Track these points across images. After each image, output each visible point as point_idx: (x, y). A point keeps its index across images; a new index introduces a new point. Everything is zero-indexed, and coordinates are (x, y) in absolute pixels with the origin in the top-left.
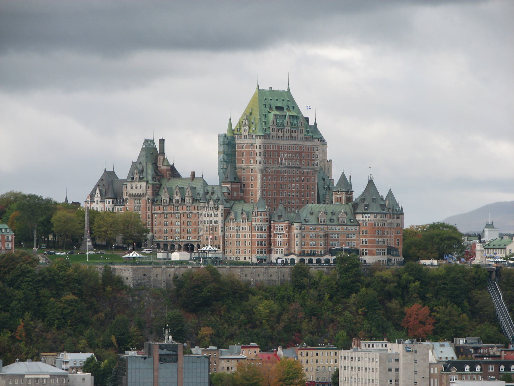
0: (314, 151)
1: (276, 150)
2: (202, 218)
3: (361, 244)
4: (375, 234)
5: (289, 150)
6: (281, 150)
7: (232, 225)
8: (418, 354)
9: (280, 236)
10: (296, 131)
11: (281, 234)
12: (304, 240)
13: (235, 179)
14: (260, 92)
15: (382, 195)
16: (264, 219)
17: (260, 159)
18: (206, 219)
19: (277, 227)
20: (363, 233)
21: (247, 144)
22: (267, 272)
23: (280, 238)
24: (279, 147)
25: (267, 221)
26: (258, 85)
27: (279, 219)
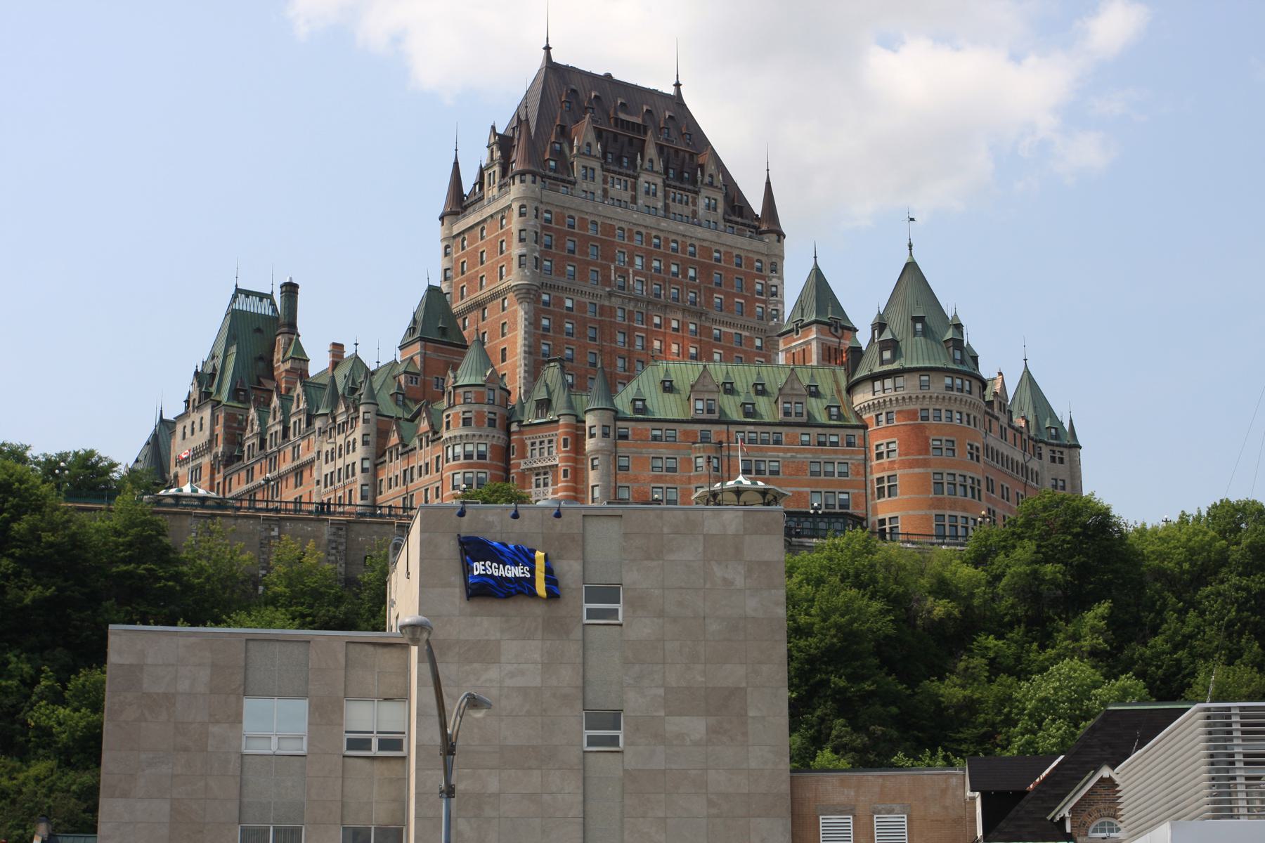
0: (764, 273)
1: (599, 236)
2: (320, 468)
4: (927, 452)
5: (652, 248)
6: (617, 240)
7: (394, 468)
9: (542, 477)
10: (690, 200)
11: (545, 471)
15: (956, 315)
16: (480, 415)
17: (524, 251)
18: (327, 469)
19: (533, 444)
20: (879, 456)
21: (492, 216)
22: (343, 540)
23: (542, 489)
24: (609, 230)
26: (548, 48)
27: (537, 418)
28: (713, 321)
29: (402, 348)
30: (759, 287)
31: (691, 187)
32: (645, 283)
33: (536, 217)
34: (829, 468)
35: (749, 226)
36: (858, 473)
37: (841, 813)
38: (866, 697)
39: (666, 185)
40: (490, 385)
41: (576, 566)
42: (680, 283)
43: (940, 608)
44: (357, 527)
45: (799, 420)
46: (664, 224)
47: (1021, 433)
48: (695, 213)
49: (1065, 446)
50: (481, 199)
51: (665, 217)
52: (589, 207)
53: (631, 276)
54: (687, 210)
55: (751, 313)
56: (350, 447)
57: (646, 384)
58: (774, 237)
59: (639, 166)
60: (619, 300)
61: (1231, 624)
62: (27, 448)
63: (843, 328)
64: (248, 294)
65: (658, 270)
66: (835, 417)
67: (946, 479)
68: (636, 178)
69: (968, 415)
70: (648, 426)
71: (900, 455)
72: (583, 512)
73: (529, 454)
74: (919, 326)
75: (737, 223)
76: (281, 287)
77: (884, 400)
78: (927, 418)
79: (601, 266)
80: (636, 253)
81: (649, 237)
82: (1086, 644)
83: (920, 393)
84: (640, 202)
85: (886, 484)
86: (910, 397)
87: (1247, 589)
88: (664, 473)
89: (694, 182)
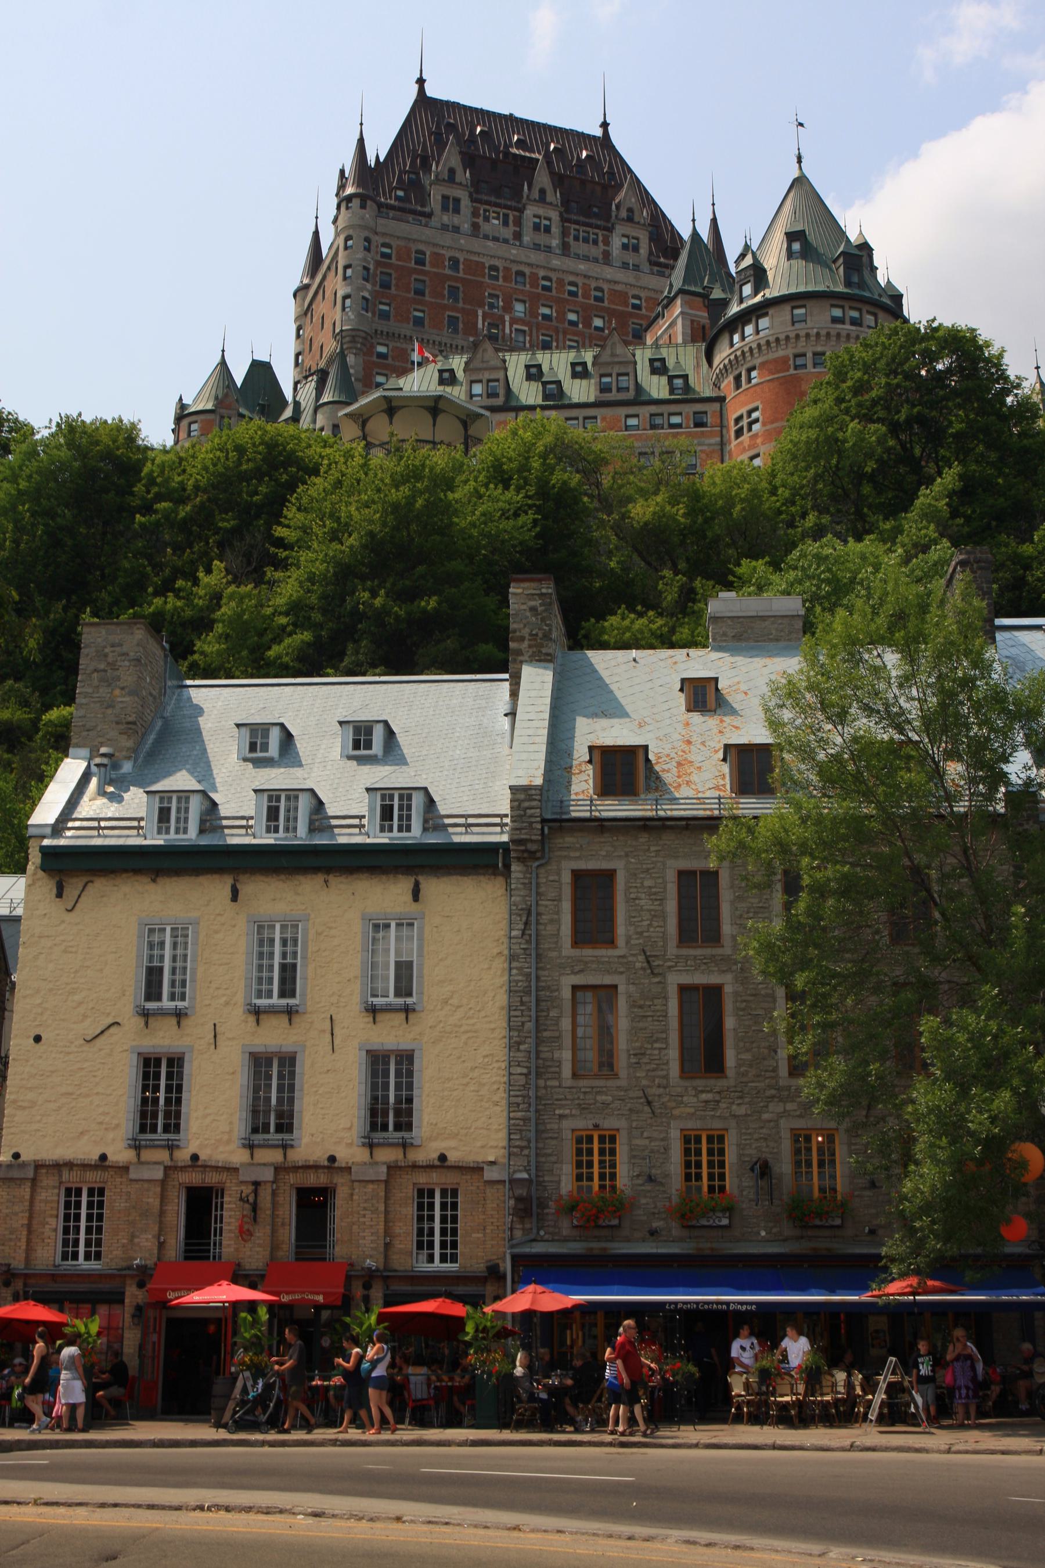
1: (461, 274)
10: (600, 238)
20: (739, 433)
24: (474, 267)
26: (421, 81)
32: (528, 332)
33: (367, 249)
39: (563, 220)
46: (556, 262)
48: (607, 255)
52: (447, 239)
53: (507, 324)
54: (596, 251)
59: (525, 196)
65: (545, 317)
66: (680, 391)
68: (521, 211)
71: (764, 424)
74: (796, 246)
77: (743, 352)
80: (515, 296)
81: (534, 277)
83: (790, 330)
84: (526, 239)
86: (777, 340)
89: (608, 217)
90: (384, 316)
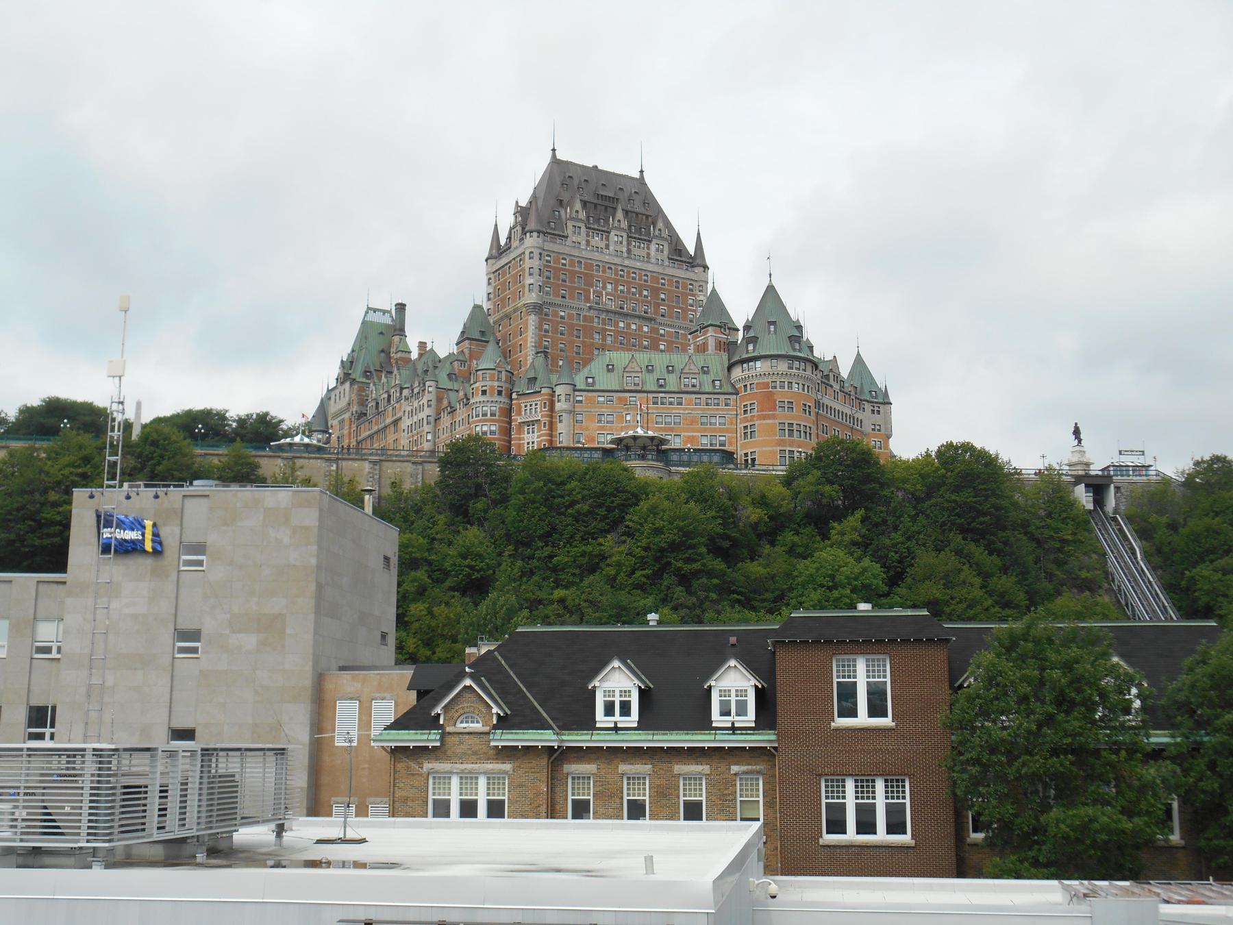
3: (741, 440)
5: (619, 277)
8: (217, 572)
9: (531, 427)
11: (533, 423)
12: (581, 428)
13: (482, 333)
14: (557, 165)
17: (532, 281)
18: (409, 422)
19: (526, 406)
20: (745, 412)
21: (514, 259)
24: (589, 266)
25: (500, 393)
26: (554, 150)
28: (660, 324)
29: (457, 344)
30: (691, 301)
31: (647, 238)
33: (540, 259)
34: (713, 420)
35: (685, 262)
36: (732, 424)
37: (351, 699)
38: (696, 574)
39: (629, 237)
40: (499, 369)
41: (177, 531)
42: (637, 300)
43: (752, 514)
44: (386, 464)
45: (694, 389)
46: (627, 262)
47: (850, 395)
48: (648, 254)
49: (880, 403)
50: (510, 248)
51: (628, 257)
54: (644, 253)
55: (685, 319)
56: (421, 408)
57: (596, 368)
58: (702, 269)
60: (596, 312)
61: (944, 524)
62: (227, 411)
63: (729, 329)
64: (375, 310)
65: (622, 291)
67: (795, 427)
68: (609, 233)
69: (804, 385)
70: (596, 394)
72: (184, 494)
73: (523, 413)
75: (677, 260)
76: (396, 305)
78: (775, 387)
79: (584, 290)
81: (616, 270)
82: (847, 538)
84: (611, 248)
85: (749, 430)
87: (955, 501)
88: (605, 424)
90: (548, 293)
